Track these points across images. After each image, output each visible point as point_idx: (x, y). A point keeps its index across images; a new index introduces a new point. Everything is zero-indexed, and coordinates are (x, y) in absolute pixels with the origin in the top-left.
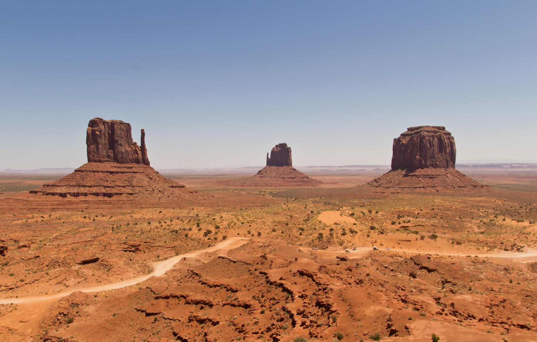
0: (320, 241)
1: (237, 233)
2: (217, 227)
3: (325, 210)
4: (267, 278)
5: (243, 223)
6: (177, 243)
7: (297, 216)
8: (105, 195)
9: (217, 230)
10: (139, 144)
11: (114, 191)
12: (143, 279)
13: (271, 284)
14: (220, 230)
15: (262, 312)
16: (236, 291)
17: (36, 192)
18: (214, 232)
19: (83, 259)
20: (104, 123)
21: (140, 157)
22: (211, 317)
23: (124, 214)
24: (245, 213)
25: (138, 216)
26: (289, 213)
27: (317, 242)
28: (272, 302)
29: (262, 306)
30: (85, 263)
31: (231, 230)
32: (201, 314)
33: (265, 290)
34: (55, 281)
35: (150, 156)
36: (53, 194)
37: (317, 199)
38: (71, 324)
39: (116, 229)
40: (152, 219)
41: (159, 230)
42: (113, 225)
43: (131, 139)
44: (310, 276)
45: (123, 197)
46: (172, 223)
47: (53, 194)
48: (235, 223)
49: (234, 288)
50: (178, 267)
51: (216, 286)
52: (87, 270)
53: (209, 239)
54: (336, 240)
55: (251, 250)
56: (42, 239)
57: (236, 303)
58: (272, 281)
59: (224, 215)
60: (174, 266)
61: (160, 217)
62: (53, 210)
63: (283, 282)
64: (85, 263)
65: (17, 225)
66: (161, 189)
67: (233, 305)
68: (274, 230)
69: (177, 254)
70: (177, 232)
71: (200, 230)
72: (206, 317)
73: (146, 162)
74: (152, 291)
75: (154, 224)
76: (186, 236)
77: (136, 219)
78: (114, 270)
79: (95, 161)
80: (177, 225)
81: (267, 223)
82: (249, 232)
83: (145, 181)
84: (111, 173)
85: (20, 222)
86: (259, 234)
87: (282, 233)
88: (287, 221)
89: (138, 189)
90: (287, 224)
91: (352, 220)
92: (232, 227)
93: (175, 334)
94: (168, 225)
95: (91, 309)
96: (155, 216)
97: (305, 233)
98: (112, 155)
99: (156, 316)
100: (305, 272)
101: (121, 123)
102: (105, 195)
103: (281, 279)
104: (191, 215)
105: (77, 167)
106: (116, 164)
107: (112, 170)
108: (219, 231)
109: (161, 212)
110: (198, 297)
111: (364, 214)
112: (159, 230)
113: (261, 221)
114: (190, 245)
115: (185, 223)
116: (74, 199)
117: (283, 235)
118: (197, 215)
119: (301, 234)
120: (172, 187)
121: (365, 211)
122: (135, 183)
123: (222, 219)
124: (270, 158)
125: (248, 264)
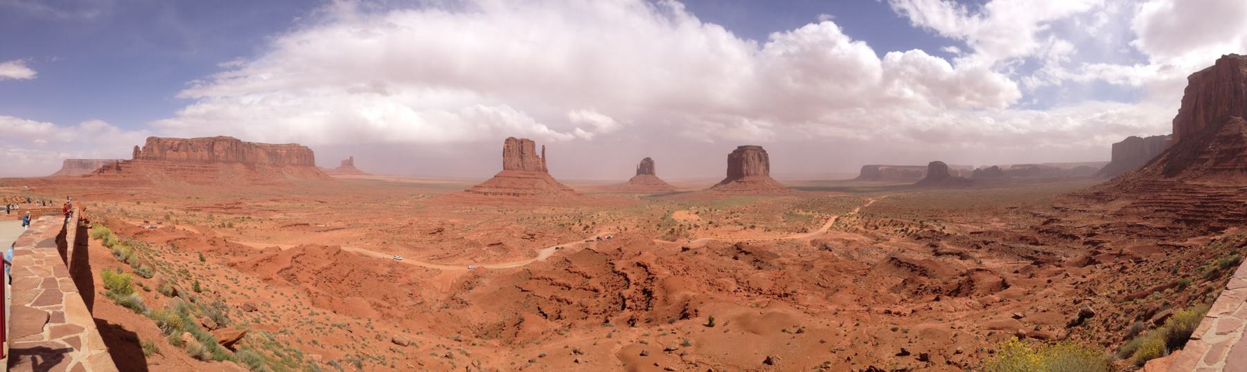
2: (594, 223)
3: (679, 210)
4: (613, 268)
6: (561, 235)
8: (514, 194)
10: (541, 157)
11: (521, 192)
12: (529, 261)
13: (616, 272)
15: (604, 296)
16: (590, 278)
17: (468, 191)
18: (591, 227)
19: (491, 243)
20: (516, 140)
21: (541, 167)
22: (567, 298)
24: (617, 212)
27: (669, 236)
28: (614, 288)
29: (606, 291)
30: (491, 245)
32: (561, 295)
33: (610, 278)
34: (467, 258)
35: (548, 165)
36: (479, 193)
37: (673, 201)
38: (471, 291)
39: (519, 221)
43: (535, 153)
44: (645, 267)
45: (527, 197)
47: (479, 193)
49: (588, 275)
51: (575, 272)
52: (491, 252)
54: (683, 233)
55: (615, 242)
56: (469, 225)
57: (587, 288)
59: (600, 214)
62: (479, 204)
65: (455, 213)
66: (555, 192)
67: (585, 289)
68: (638, 226)
70: (563, 226)
71: (581, 225)
72: (563, 297)
73: (545, 170)
74: (529, 272)
76: (570, 229)
77: (535, 214)
78: (509, 253)
79: (508, 169)
80: (565, 220)
81: (633, 221)
82: (618, 228)
83: (544, 185)
84: (520, 178)
85: (456, 211)
86: (626, 229)
89: (538, 191)
90: (648, 221)
91: (698, 217)
93: (539, 309)
95: (486, 282)
96: (549, 213)
97: (662, 228)
98: (520, 165)
99: (528, 293)
100: (642, 264)
101: (528, 140)
102: (514, 194)
103: (623, 269)
104: (577, 212)
105: (496, 174)
106: (523, 172)
107: (520, 176)
110: (561, 281)
111: (706, 211)
116: (493, 197)
118: (581, 213)
119: (658, 229)
120: (564, 190)
121: (707, 210)
122: (536, 186)
125: (606, 254)
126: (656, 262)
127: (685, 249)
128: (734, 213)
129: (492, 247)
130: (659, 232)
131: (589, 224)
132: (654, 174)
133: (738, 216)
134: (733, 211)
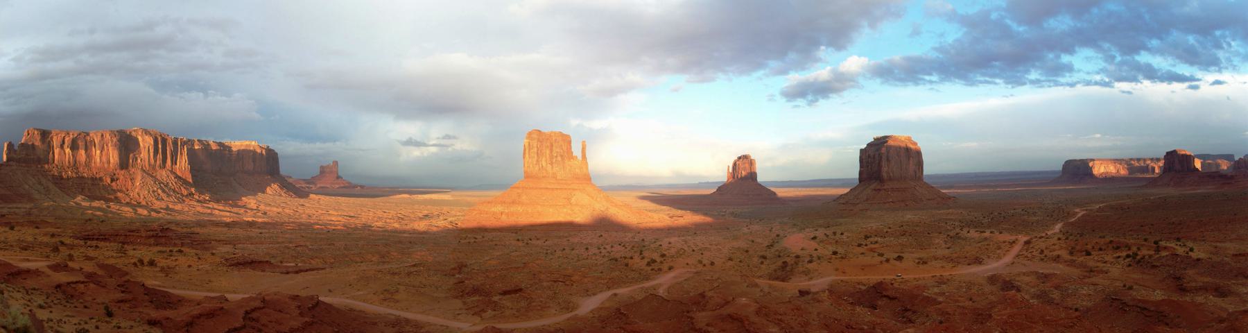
0: (783, 271)
1: (686, 262)
2: (663, 256)
5: (693, 251)
7: (760, 240)
9: (662, 259)
10: (580, 157)
14: (666, 258)
23: (560, 237)
25: (576, 240)
26: (751, 238)
30: (505, 293)
31: (680, 259)
40: (591, 244)
41: (597, 257)
42: (547, 250)
46: (613, 249)
48: (685, 251)
50: (607, 305)
53: (652, 270)
58: (697, 328)
60: (602, 303)
61: (600, 241)
63: (710, 329)
64: (505, 293)
68: (730, 259)
69: (609, 288)
70: (616, 260)
71: (643, 258)
75: (593, 250)
87: (740, 262)
88: (748, 248)
92: (681, 255)
94: (608, 252)
103: (708, 325)
104: (635, 240)
108: (664, 260)
109: (601, 236)
112: (597, 257)
113: (715, 247)
114: (629, 277)
115: (627, 250)
117: (742, 264)
118: (643, 240)
119: (762, 263)
122: (573, 201)
123: (670, 245)
124: (731, 170)
126: (758, 313)
127: (803, 293)
128: (871, 237)
129: (508, 296)
130: (762, 266)
131: (656, 256)
132: (756, 179)
133: (876, 242)
134: (869, 235)
